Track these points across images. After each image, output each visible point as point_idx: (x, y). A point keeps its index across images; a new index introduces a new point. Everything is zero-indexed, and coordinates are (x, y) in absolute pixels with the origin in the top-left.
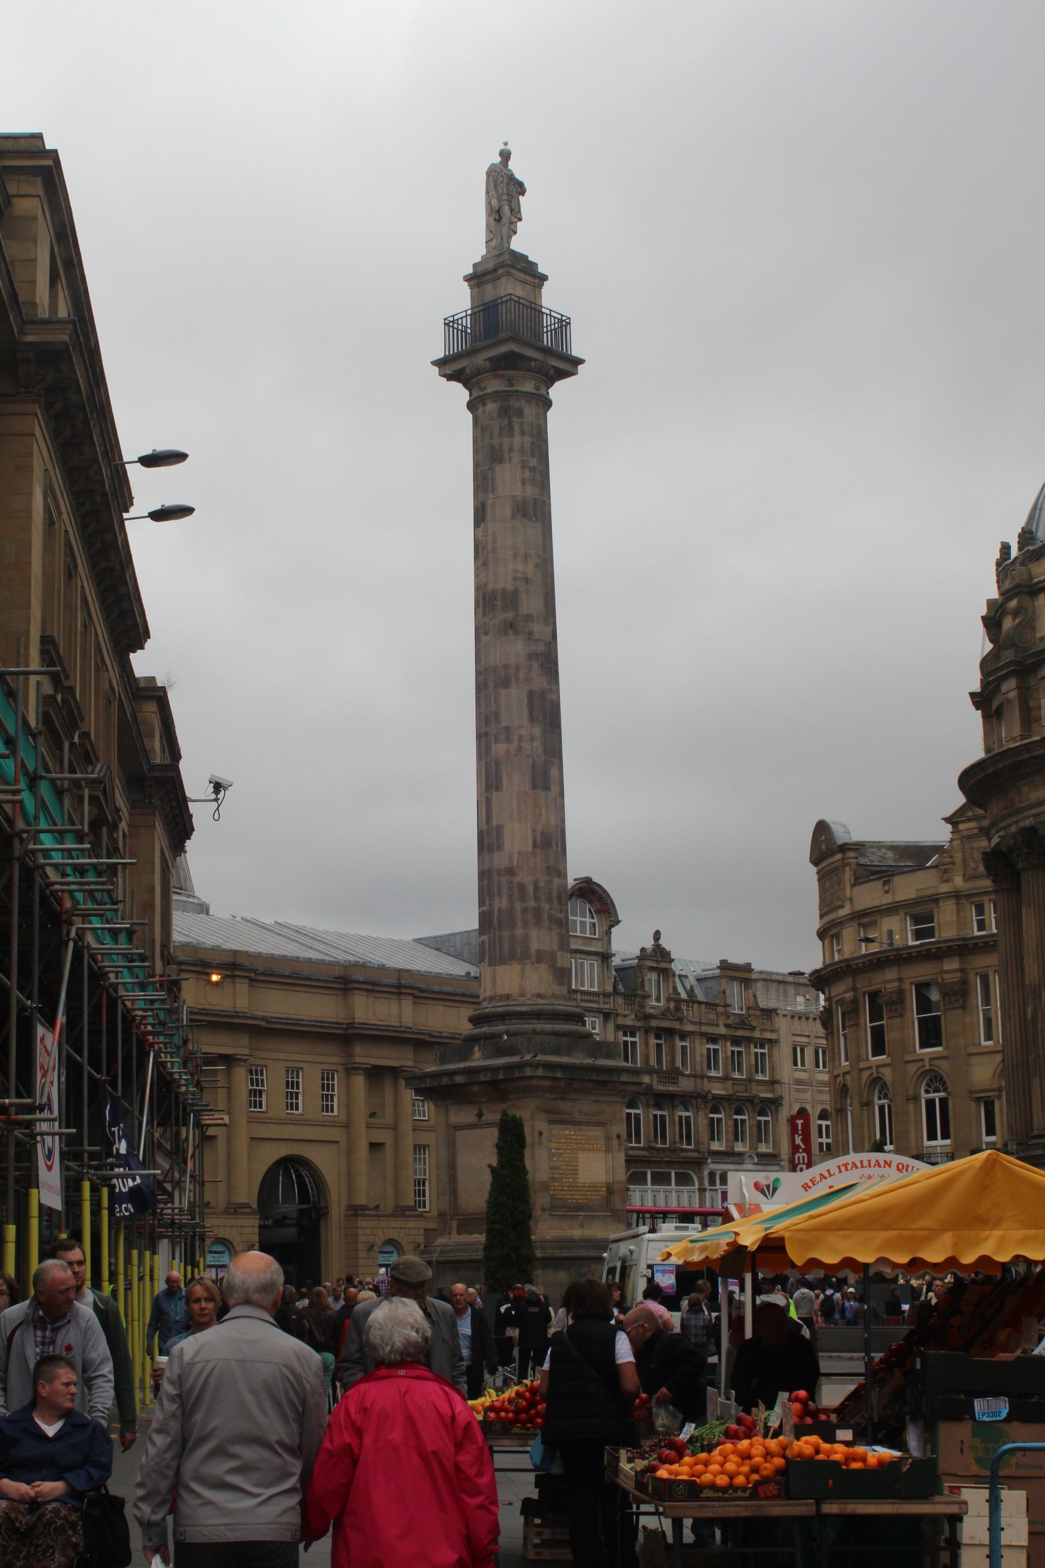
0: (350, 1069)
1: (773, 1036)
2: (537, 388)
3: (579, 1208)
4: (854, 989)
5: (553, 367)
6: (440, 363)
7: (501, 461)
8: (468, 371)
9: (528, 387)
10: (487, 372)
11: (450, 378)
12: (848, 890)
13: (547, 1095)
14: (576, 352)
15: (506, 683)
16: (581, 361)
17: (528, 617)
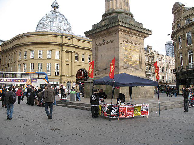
1: (154, 56)
3: (132, 67)
4: (184, 33)
12: (182, 14)
13: (123, 33)
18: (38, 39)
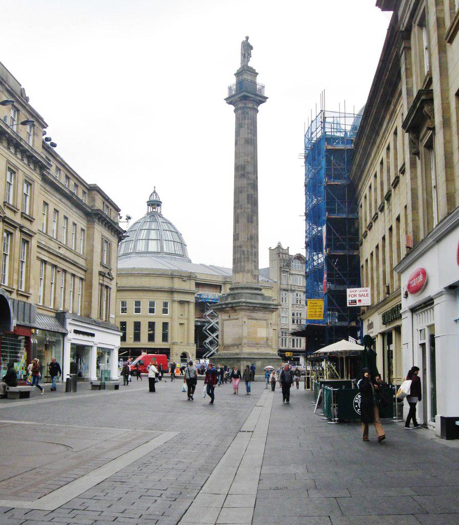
0: (173, 301)
2: (253, 106)
6: (226, 99)
7: (242, 127)
9: (250, 105)
11: (230, 103)
14: (266, 95)
15: (241, 192)
16: (267, 98)
17: (248, 173)
18: (133, 282)
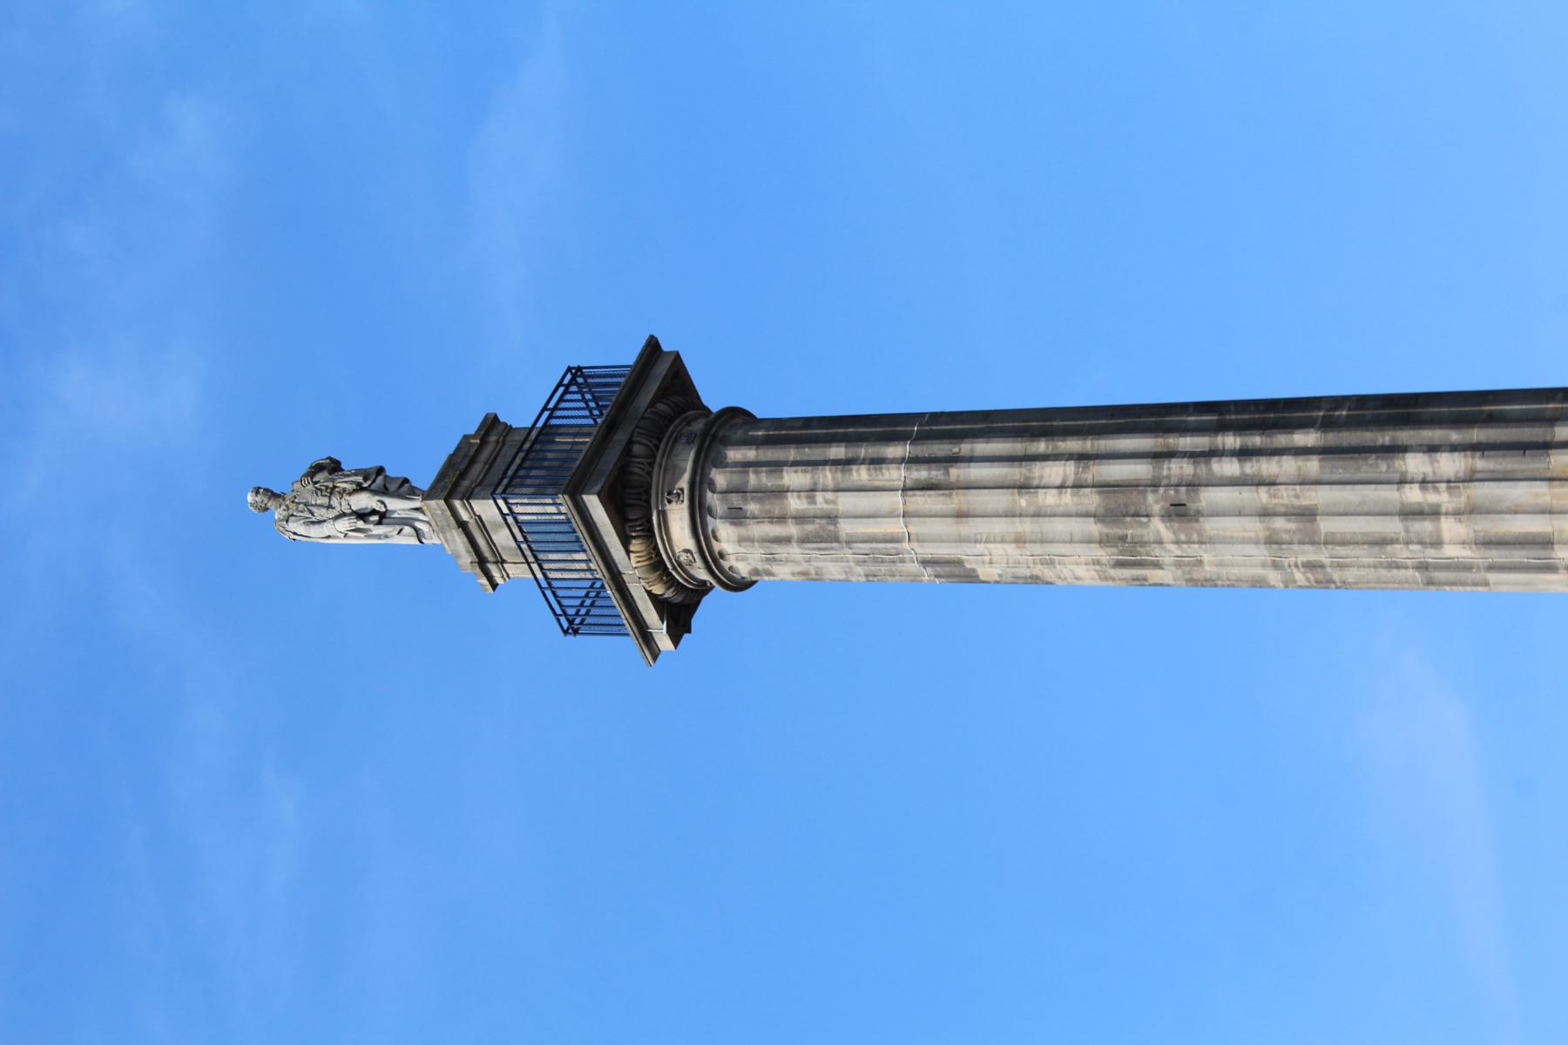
5: (652, 404)
8: (658, 589)
10: (656, 548)
14: (627, 355)
16: (653, 347)
